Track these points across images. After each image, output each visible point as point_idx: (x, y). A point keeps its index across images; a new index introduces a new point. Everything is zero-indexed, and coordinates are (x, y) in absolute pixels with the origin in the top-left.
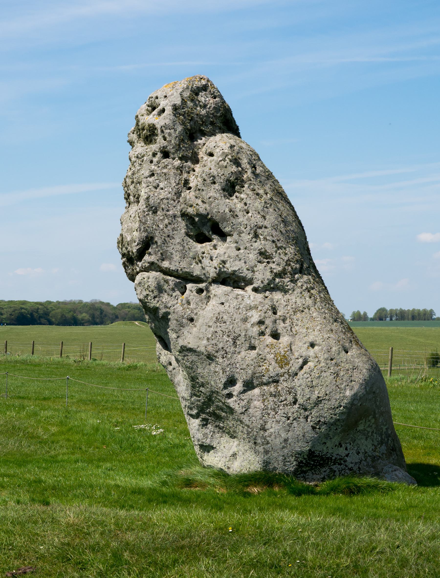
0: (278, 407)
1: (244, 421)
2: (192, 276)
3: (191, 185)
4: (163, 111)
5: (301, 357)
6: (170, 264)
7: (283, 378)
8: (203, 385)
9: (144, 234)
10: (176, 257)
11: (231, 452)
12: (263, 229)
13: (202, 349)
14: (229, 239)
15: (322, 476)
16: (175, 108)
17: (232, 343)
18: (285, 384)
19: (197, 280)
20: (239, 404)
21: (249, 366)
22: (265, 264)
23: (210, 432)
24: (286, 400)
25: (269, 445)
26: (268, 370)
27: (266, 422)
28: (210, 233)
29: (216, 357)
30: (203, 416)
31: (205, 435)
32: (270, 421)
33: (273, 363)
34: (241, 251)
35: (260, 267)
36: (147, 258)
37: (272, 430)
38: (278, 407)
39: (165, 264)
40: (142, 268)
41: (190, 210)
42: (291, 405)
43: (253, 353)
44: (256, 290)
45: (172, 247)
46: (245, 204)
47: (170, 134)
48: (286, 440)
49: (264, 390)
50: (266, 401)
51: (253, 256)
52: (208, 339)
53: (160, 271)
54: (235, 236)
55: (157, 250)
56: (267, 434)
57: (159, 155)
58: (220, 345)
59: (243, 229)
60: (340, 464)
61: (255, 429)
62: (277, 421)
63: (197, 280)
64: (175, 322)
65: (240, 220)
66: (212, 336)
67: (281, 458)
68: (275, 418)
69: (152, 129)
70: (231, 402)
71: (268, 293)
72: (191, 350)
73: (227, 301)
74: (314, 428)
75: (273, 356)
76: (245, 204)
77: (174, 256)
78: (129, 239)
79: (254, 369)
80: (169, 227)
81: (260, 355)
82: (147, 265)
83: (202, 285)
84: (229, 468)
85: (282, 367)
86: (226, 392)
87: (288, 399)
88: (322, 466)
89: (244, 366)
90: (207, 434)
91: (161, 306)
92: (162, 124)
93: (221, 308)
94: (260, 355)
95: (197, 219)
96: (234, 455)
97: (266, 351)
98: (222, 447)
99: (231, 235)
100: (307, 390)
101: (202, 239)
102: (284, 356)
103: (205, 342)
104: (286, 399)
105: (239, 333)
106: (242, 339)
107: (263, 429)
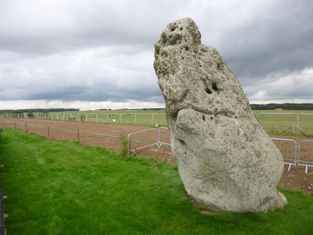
0: (256, 177)
1: (238, 186)
2: (207, 111)
3: (201, 64)
4: (181, 29)
5: (265, 152)
6: (198, 104)
7: (259, 163)
8: (212, 166)
9: (185, 89)
10: (201, 101)
11: (219, 195)
12: (236, 87)
13: (220, 151)
14: (221, 92)
15: (267, 206)
16: (187, 28)
17: (233, 146)
18: (260, 166)
19: (210, 113)
20: (237, 178)
21: (242, 158)
22: (240, 105)
23: (207, 186)
24: (260, 174)
25: (250, 196)
26: (252, 160)
27: (249, 186)
28: (212, 89)
29: (226, 154)
30: (205, 179)
31: (203, 187)
32: (251, 185)
33: (254, 156)
34: (229, 98)
35: (238, 106)
36: (186, 101)
37: (252, 189)
38: (256, 177)
39: (195, 105)
40: (183, 107)
41: (204, 77)
42: (262, 176)
43: (244, 151)
44: (236, 117)
45: (198, 96)
46: (226, 75)
47: (189, 39)
48: (258, 194)
49: (249, 169)
50: (250, 175)
51: (234, 101)
52: (222, 145)
53: (192, 108)
54: (225, 91)
55: (190, 97)
56: (249, 191)
57: (184, 49)
58: (228, 148)
59: (228, 87)
60: (273, 199)
61: (244, 190)
62: (255, 185)
63: (210, 113)
64: (202, 135)
65: (227, 83)
66: (224, 143)
67: (254, 202)
68: (254, 183)
69: (179, 37)
70: (231, 176)
71: (242, 119)
72: (211, 150)
73: (228, 124)
74: (270, 186)
75: (254, 152)
76: (226, 75)
77: (199, 100)
78: (175, 91)
79: (245, 159)
80: (196, 85)
81: (248, 152)
82: (186, 105)
83: (213, 116)
84: (216, 202)
85: (259, 158)
86: (230, 171)
87: (261, 173)
88: (267, 201)
89: (240, 158)
90: (205, 186)
91: (196, 128)
92: (184, 33)
93: (225, 128)
94: (248, 152)
95: (207, 81)
96: (220, 197)
97: (250, 150)
98: (213, 193)
99: (222, 90)
100: (269, 168)
101: (209, 92)
102: (259, 152)
103: (221, 146)
104: (260, 174)
105: (237, 141)
106: (238, 144)
107: (248, 189)
